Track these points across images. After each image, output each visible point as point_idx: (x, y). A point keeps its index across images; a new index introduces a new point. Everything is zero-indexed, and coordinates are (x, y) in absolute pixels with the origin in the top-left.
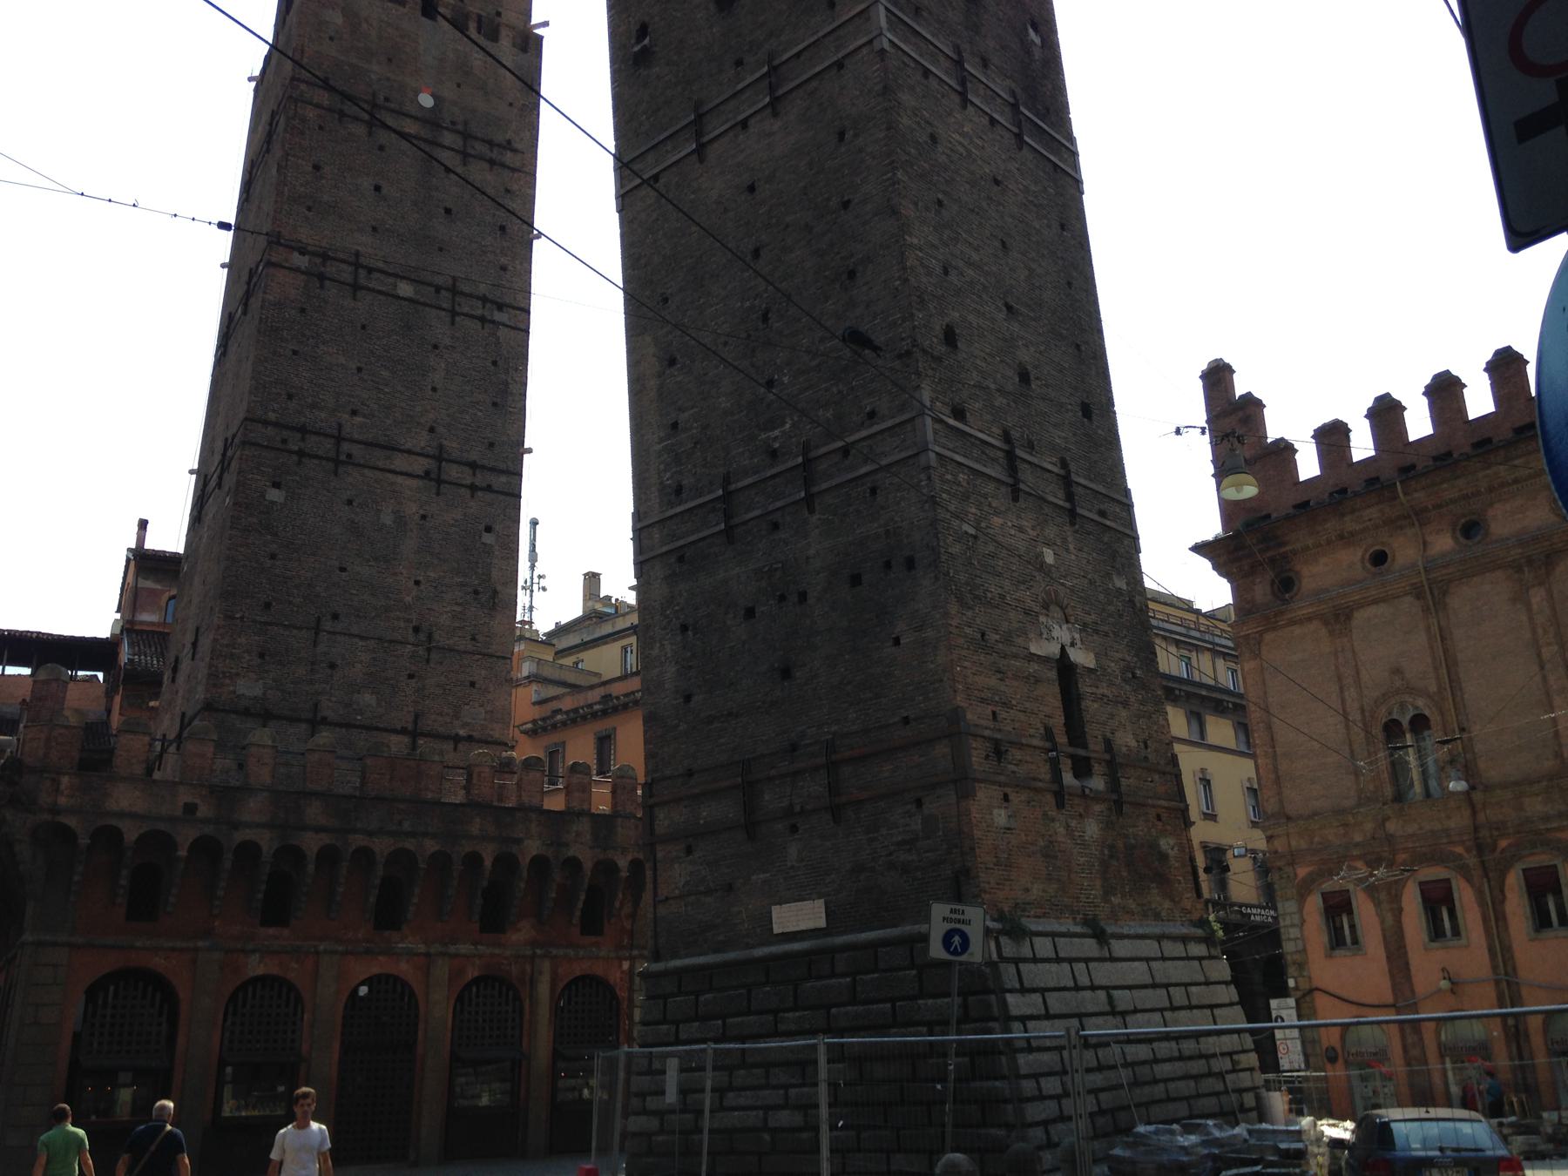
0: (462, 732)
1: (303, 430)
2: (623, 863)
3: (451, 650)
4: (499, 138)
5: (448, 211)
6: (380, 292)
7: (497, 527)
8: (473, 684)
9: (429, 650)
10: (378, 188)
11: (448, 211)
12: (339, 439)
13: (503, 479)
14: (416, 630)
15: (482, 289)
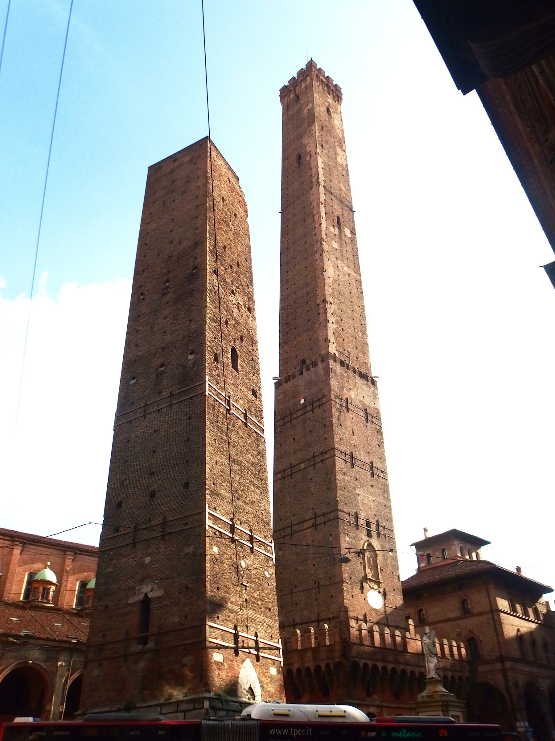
0: (331, 616)
1: (284, 529)
2: (323, 666)
3: (325, 586)
4: (320, 396)
5: (310, 431)
6: (297, 471)
7: (333, 533)
8: (332, 596)
9: (319, 589)
10: (294, 439)
11: (310, 431)
12: (291, 526)
13: (333, 514)
14: (315, 582)
15: (321, 450)
